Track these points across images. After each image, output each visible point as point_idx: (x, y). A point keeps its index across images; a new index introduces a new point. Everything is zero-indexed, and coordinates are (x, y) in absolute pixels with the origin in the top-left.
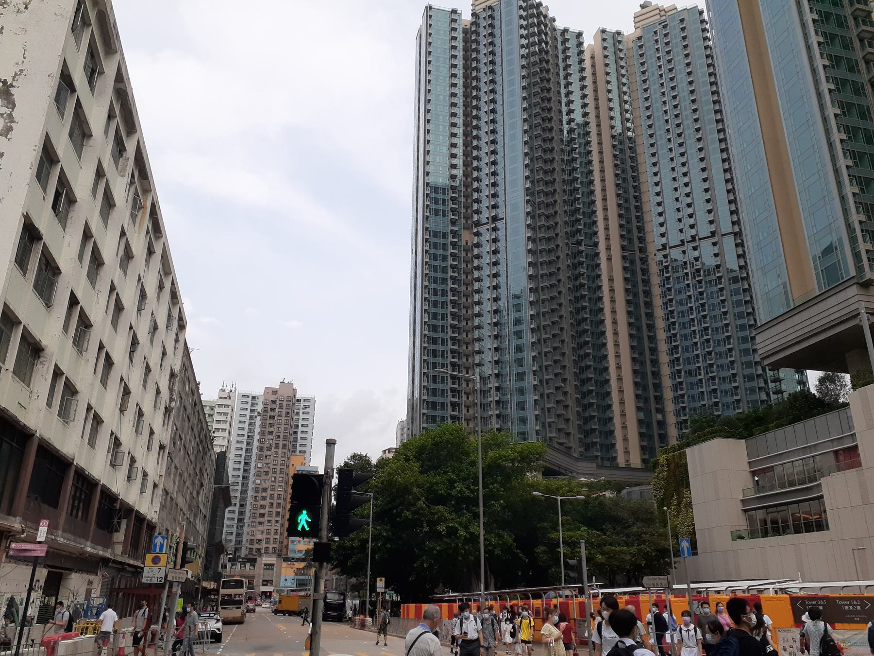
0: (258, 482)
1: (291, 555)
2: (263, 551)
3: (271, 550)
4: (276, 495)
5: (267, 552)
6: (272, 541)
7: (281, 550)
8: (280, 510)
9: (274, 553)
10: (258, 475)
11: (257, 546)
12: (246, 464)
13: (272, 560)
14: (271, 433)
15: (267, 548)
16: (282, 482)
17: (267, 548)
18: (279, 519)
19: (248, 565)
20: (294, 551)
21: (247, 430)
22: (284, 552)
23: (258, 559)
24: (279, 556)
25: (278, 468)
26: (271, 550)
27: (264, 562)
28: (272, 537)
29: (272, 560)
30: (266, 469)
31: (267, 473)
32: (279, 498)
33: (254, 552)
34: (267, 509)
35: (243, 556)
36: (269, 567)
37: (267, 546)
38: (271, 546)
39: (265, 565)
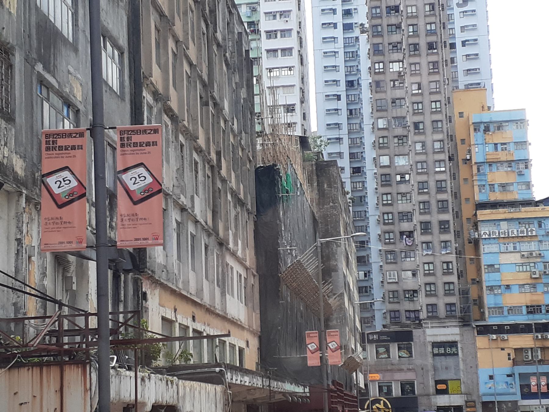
0: (385, 160)
1: (492, 320)
2: (423, 315)
3: (442, 311)
4: (432, 184)
5: (433, 315)
6: (441, 291)
7: (465, 310)
8: (448, 217)
9: (450, 316)
10: (381, 146)
11: (407, 305)
12: (350, 84)
13: (450, 332)
14: (396, 46)
15: (433, 307)
16: (442, 151)
17: (433, 307)
18: (450, 237)
19: (394, 348)
20: (499, 309)
21: (342, 69)
22: (474, 312)
23: (416, 333)
24: (465, 322)
25: (428, 119)
26: (442, 311)
27: (430, 339)
28: (441, 279)
29: (450, 332)
30: (399, 131)
31: (402, 138)
32: (440, 190)
33: (404, 320)
34: (417, 218)
35: (379, 328)
36: (446, 348)
37: (432, 300)
38: (441, 302)
39: (435, 345)
